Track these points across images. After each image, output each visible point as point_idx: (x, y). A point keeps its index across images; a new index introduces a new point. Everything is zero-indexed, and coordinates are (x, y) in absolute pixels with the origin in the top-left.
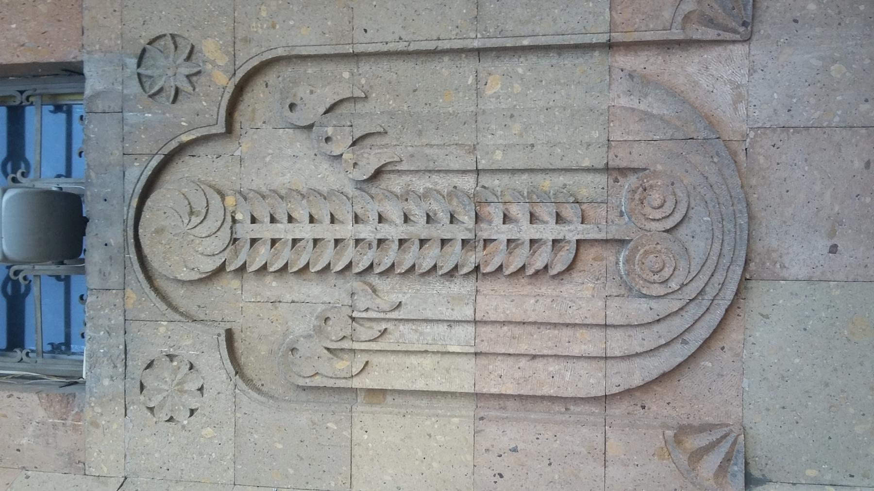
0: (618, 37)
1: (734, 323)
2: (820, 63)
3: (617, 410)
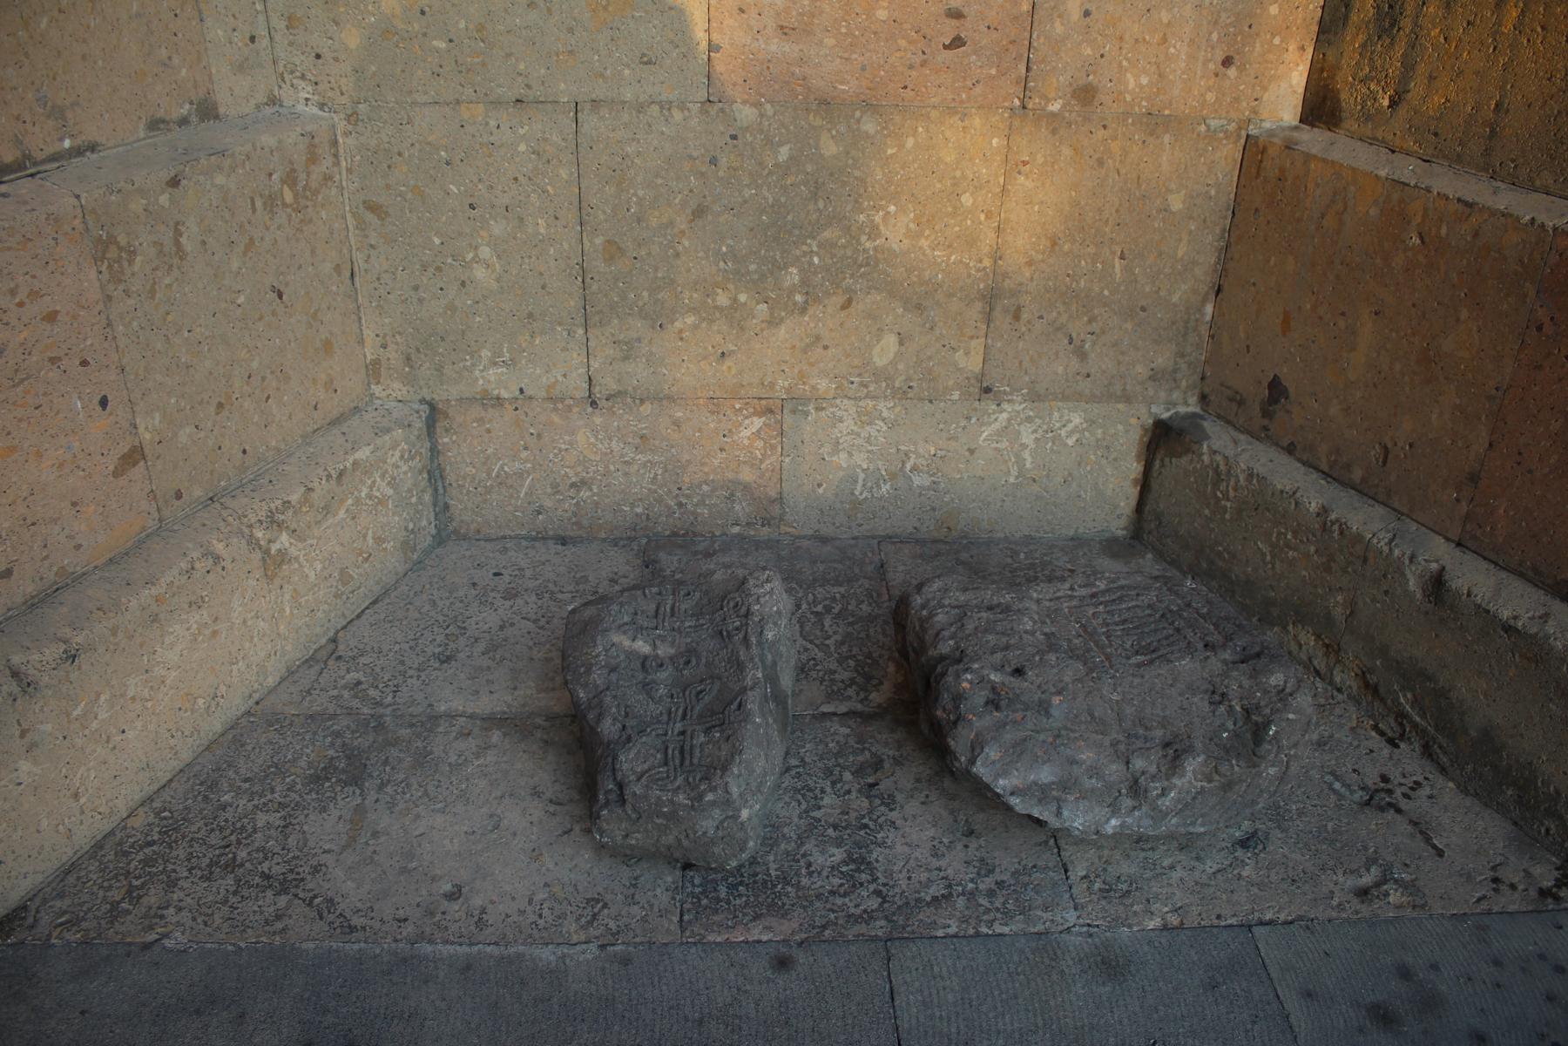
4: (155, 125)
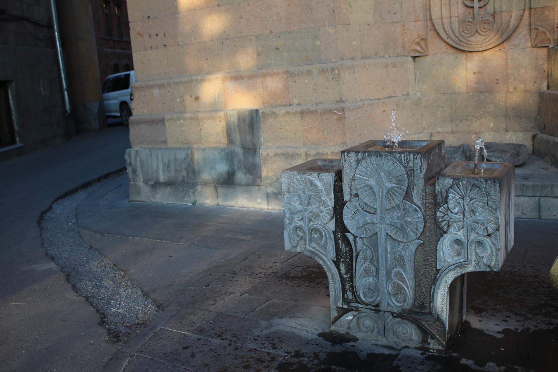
0: (533, 10)
1: (454, 51)
2: (525, 65)
3: (429, 23)
4: (403, 95)
